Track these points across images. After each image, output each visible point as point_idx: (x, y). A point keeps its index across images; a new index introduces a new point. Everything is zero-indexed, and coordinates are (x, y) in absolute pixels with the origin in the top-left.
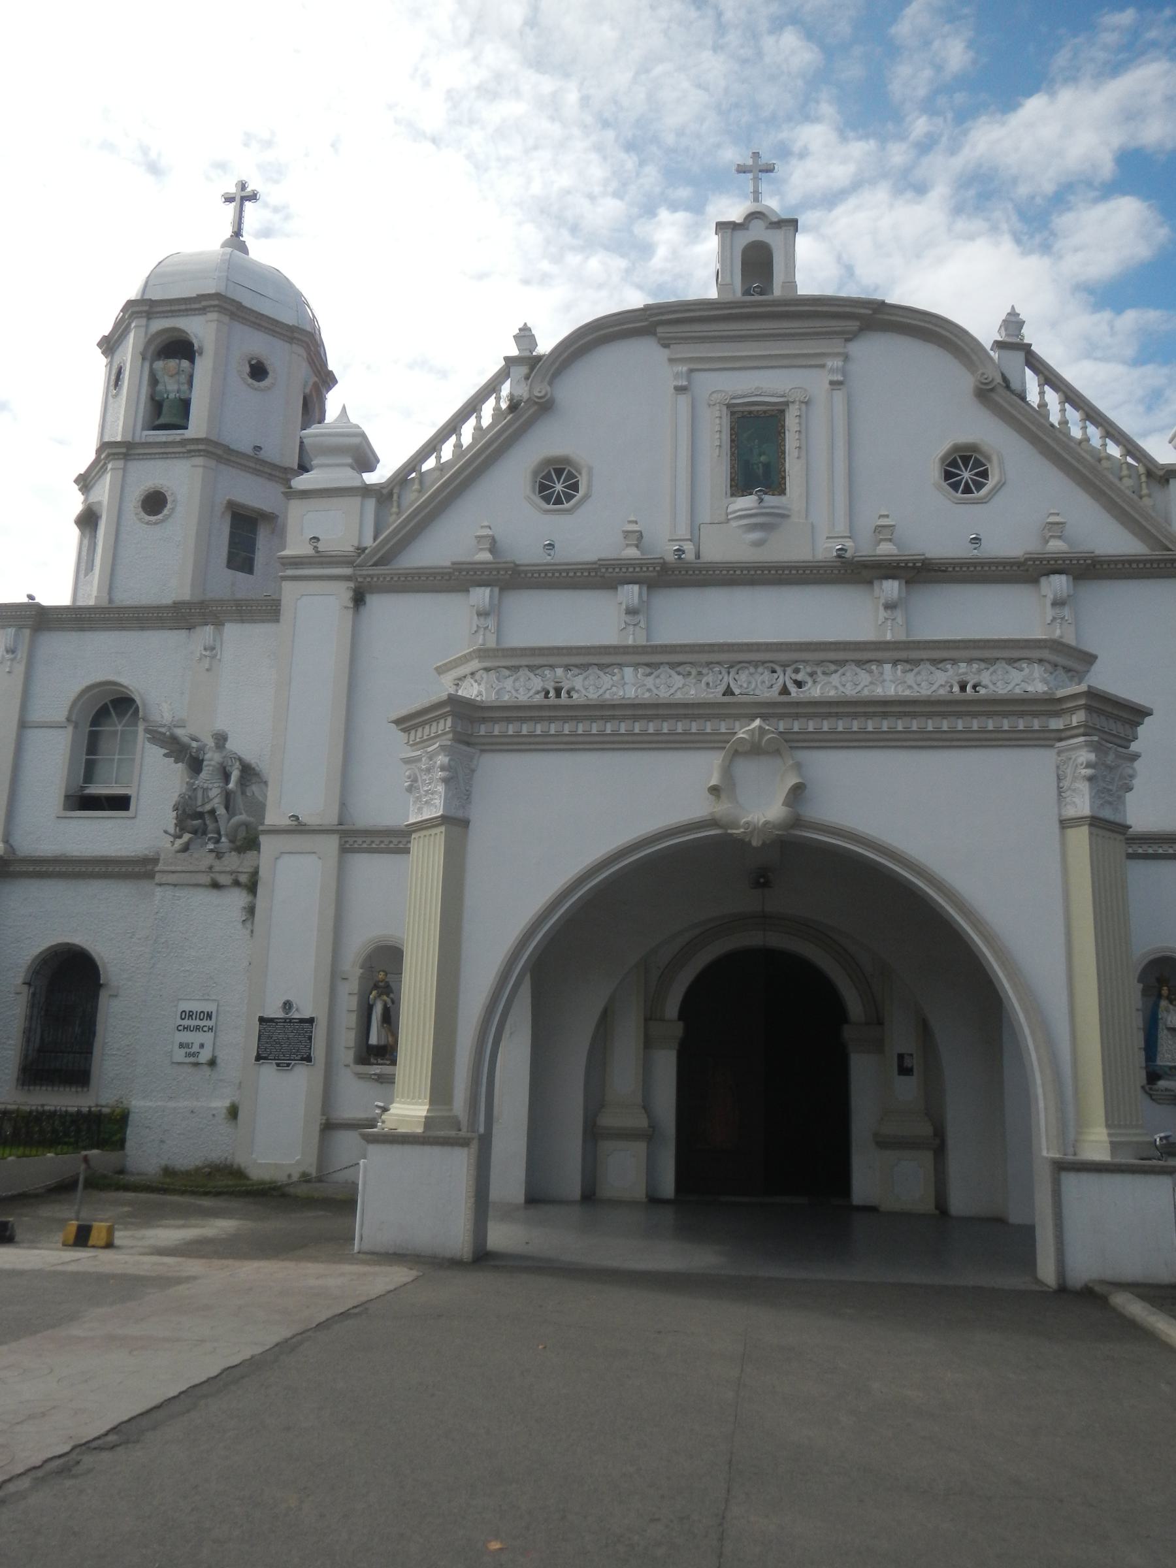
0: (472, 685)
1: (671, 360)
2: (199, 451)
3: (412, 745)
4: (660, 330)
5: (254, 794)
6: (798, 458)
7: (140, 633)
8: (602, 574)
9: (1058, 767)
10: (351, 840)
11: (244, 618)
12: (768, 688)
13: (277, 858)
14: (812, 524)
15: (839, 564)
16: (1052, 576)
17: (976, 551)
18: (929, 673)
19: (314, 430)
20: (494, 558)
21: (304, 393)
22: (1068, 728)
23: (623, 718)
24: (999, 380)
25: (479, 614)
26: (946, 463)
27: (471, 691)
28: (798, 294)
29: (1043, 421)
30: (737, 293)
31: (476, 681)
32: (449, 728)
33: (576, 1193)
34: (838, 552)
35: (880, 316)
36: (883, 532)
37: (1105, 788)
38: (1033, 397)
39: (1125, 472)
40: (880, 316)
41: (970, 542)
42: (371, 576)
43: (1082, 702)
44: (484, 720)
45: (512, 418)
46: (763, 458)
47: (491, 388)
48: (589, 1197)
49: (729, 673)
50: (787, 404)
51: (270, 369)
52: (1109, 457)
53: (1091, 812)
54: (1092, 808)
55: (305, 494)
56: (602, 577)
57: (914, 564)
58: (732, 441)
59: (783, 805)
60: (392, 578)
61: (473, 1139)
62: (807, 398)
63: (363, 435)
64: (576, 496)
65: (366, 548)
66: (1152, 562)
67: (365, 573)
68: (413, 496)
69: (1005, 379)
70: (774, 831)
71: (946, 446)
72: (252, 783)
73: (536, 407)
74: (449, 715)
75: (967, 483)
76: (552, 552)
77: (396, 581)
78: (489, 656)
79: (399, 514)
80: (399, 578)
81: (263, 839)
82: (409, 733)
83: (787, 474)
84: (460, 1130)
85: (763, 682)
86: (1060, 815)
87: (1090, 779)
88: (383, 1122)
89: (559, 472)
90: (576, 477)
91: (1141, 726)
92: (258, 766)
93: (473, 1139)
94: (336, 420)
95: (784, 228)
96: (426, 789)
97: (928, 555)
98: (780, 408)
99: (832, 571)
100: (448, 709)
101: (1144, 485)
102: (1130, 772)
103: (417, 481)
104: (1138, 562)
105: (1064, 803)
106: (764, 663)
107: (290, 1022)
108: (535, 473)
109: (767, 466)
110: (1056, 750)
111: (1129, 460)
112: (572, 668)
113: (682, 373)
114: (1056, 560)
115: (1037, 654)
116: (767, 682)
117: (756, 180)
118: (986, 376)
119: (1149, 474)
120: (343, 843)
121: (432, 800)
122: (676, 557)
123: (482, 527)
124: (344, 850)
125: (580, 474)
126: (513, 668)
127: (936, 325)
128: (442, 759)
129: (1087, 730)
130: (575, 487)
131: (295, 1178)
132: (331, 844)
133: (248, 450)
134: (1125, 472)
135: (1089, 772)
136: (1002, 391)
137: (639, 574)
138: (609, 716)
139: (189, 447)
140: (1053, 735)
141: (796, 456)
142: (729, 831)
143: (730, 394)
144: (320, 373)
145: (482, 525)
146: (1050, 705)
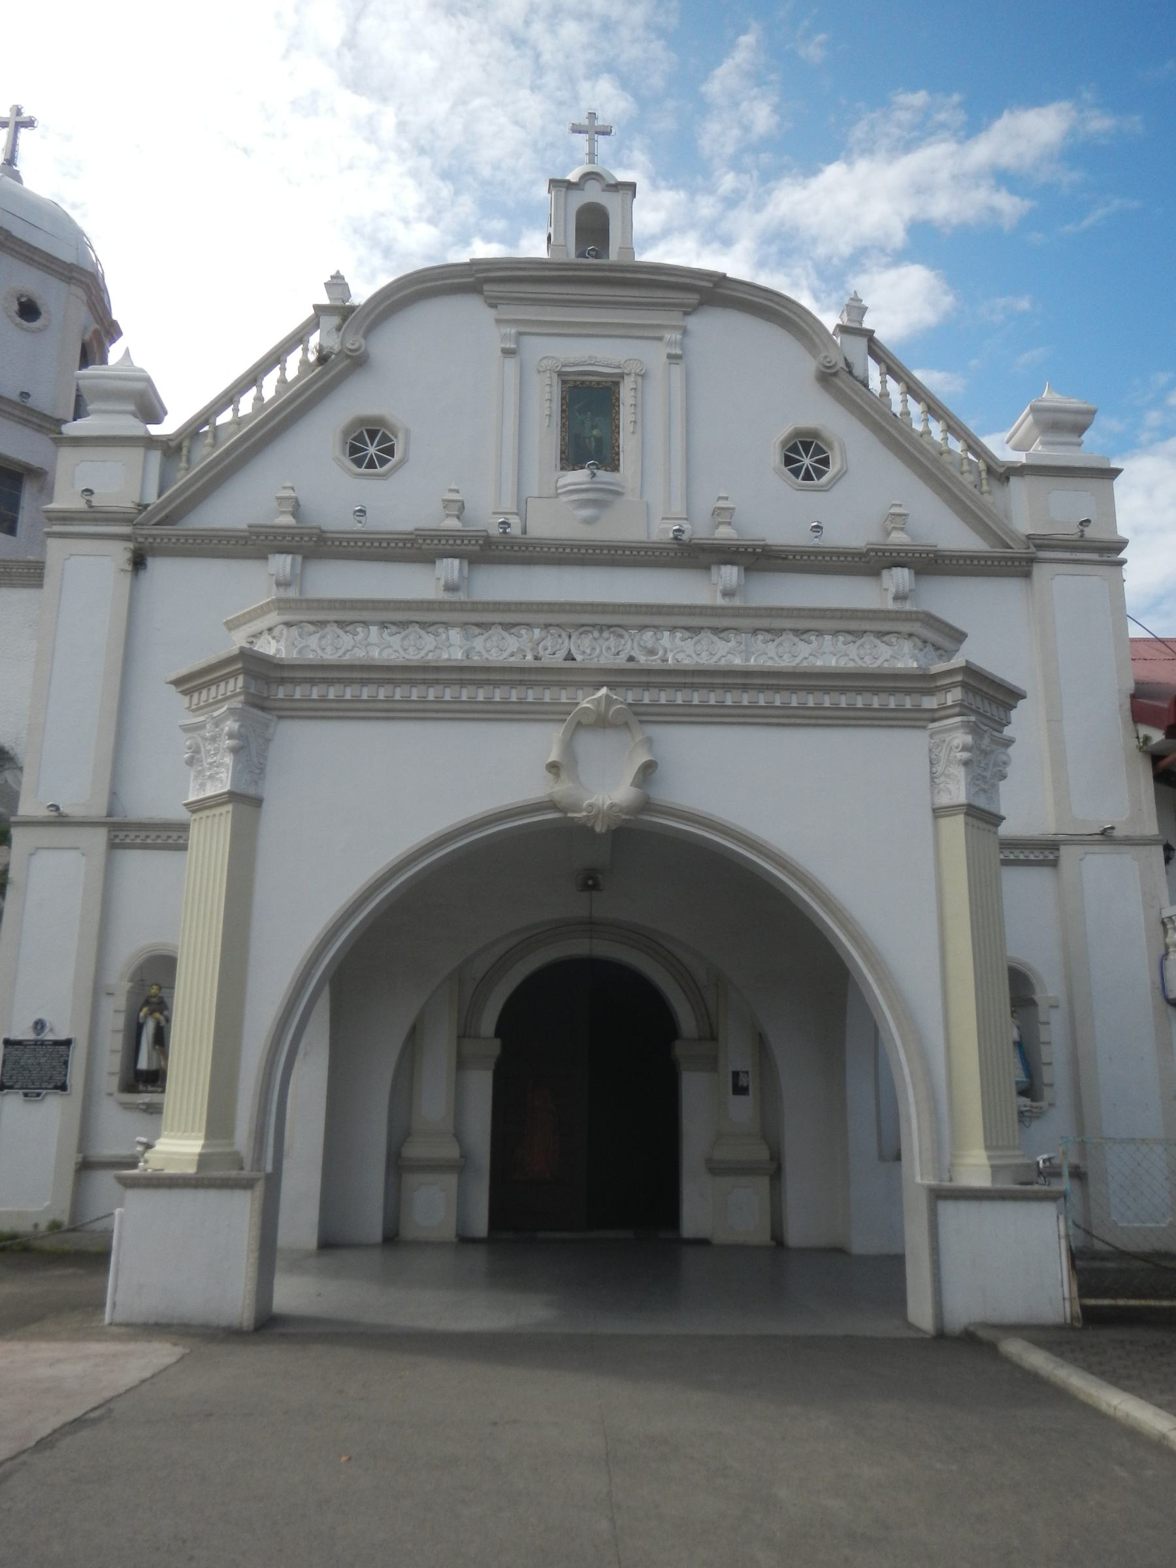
0: (269, 643)
1: (498, 321)
3: (194, 711)
4: (486, 287)
5: (6, 781)
6: (633, 433)
8: (418, 546)
9: (930, 751)
10: (122, 835)
12: (614, 655)
13: (32, 855)
14: (648, 506)
15: (676, 546)
16: (894, 568)
17: (816, 539)
18: (792, 643)
19: (91, 370)
20: (297, 522)
21: (83, 340)
22: (943, 707)
23: (448, 683)
24: (842, 364)
25: (279, 584)
26: (786, 449)
27: (269, 647)
28: (636, 260)
29: (886, 409)
30: (570, 253)
31: (274, 638)
32: (240, 688)
33: (377, 1234)
34: (676, 533)
35: (720, 290)
36: (722, 514)
37: (979, 774)
38: (875, 383)
39: (966, 467)
40: (720, 290)
41: (811, 530)
42: (154, 537)
43: (959, 678)
44: (282, 681)
45: (321, 370)
46: (595, 432)
47: (298, 338)
48: (392, 1238)
49: (570, 637)
50: (622, 376)
51: (42, 309)
52: (950, 452)
53: (966, 799)
54: (968, 797)
55: (78, 442)
56: (420, 549)
57: (755, 549)
58: (563, 411)
59: (631, 786)
60: (178, 540)
61: (259, 1179)
62: (644, 370)
63: (148, 380)
64: (390, 460)
65: (148, 505)
66: (993, 559)
67: (143, 532)
68: (206, 450)
69: (848, 364)
70: (620, 814)
71: (785, 431)
72: (5, 769)
73: (346, 362)
74: (240, 673)
75: (807, 470)
77: (183, 543)
78: (290, 608)
79: (187, 470)
80: (187, 540)
81: (16, 834)
82: (191, 697)
83: (621, 449)
84: (242, 1168)
85: (609, 648)
86: (933, 804)
87: (966, 763)
88: (146, 1162)
89: (372, 434)
90: (392, 441)
91: (1015, 710)
92: (12, 749)
93: (259, 1179)
94: (117, 363)
95: (621, 192)
96: (210, 760)
97: (769, 541)
98: (614, 379)
99: (668, 553)
100: (239, 665)
101: (984, 482)
102: (1005, 758)
103: (210, 435)
104: (979, 558)
105: (936, 791)
106: (609, 627)
107: (42, 1044)
108: (346, 432)
109: (599, 441)
110: (927, 733)
111: (971, 456)
112: (389, 625)
113: (510, 334)
114: (898, 552)
115: (905, 627)
116: (613, 649)
117: (592, 141)
118: (829, 360)
119: (990, 470)
120: (112, 838)
121: (217, 773)
122: (501, 530)
123: (284, 488)
124: (113, 846)
125: (396, 437)
126: (319, 624)
127: (778, 304)
128: (231, 725)
129: (964, 708)
130: (390, 451)
131: (43, 1226)
132: (99, 838)
133: (15, 397)
134: (966, 467)
135: (965, 755)
137: (460, 547)
138: (433, 679)
140: (926, 715)
141: (632, 430)
142: (570, 815)
143: (562, 360)
144: (101, 320)
145: (284, 485)
146: (923, 683)
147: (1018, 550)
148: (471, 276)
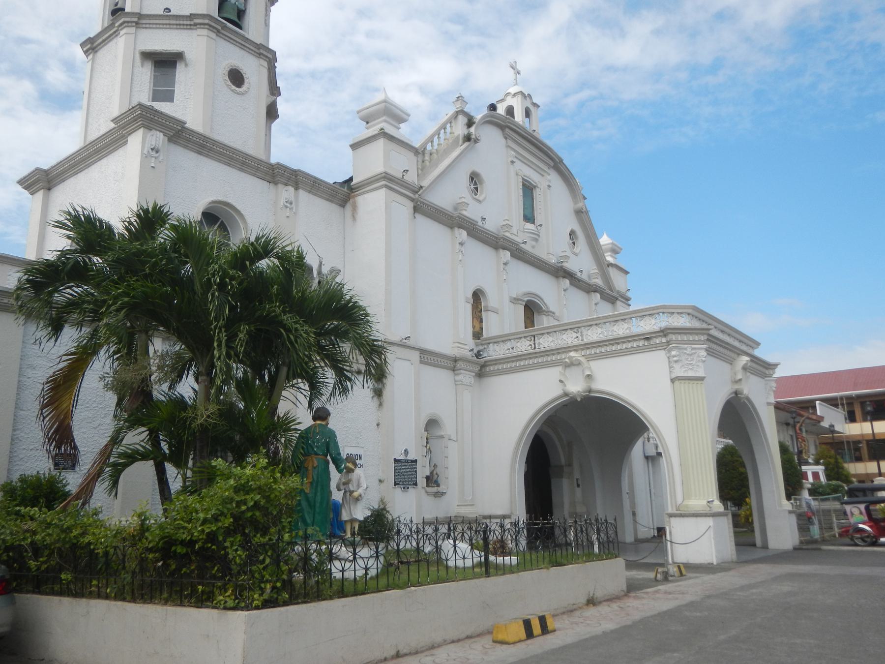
2: (266, 57)
4: (507, 130)
7: (239, 172)
11: (312, 191)
76: (484, 222)
136: (585, 214)
139: (261, 51)
147: (615, 294)
148: (505, 123)
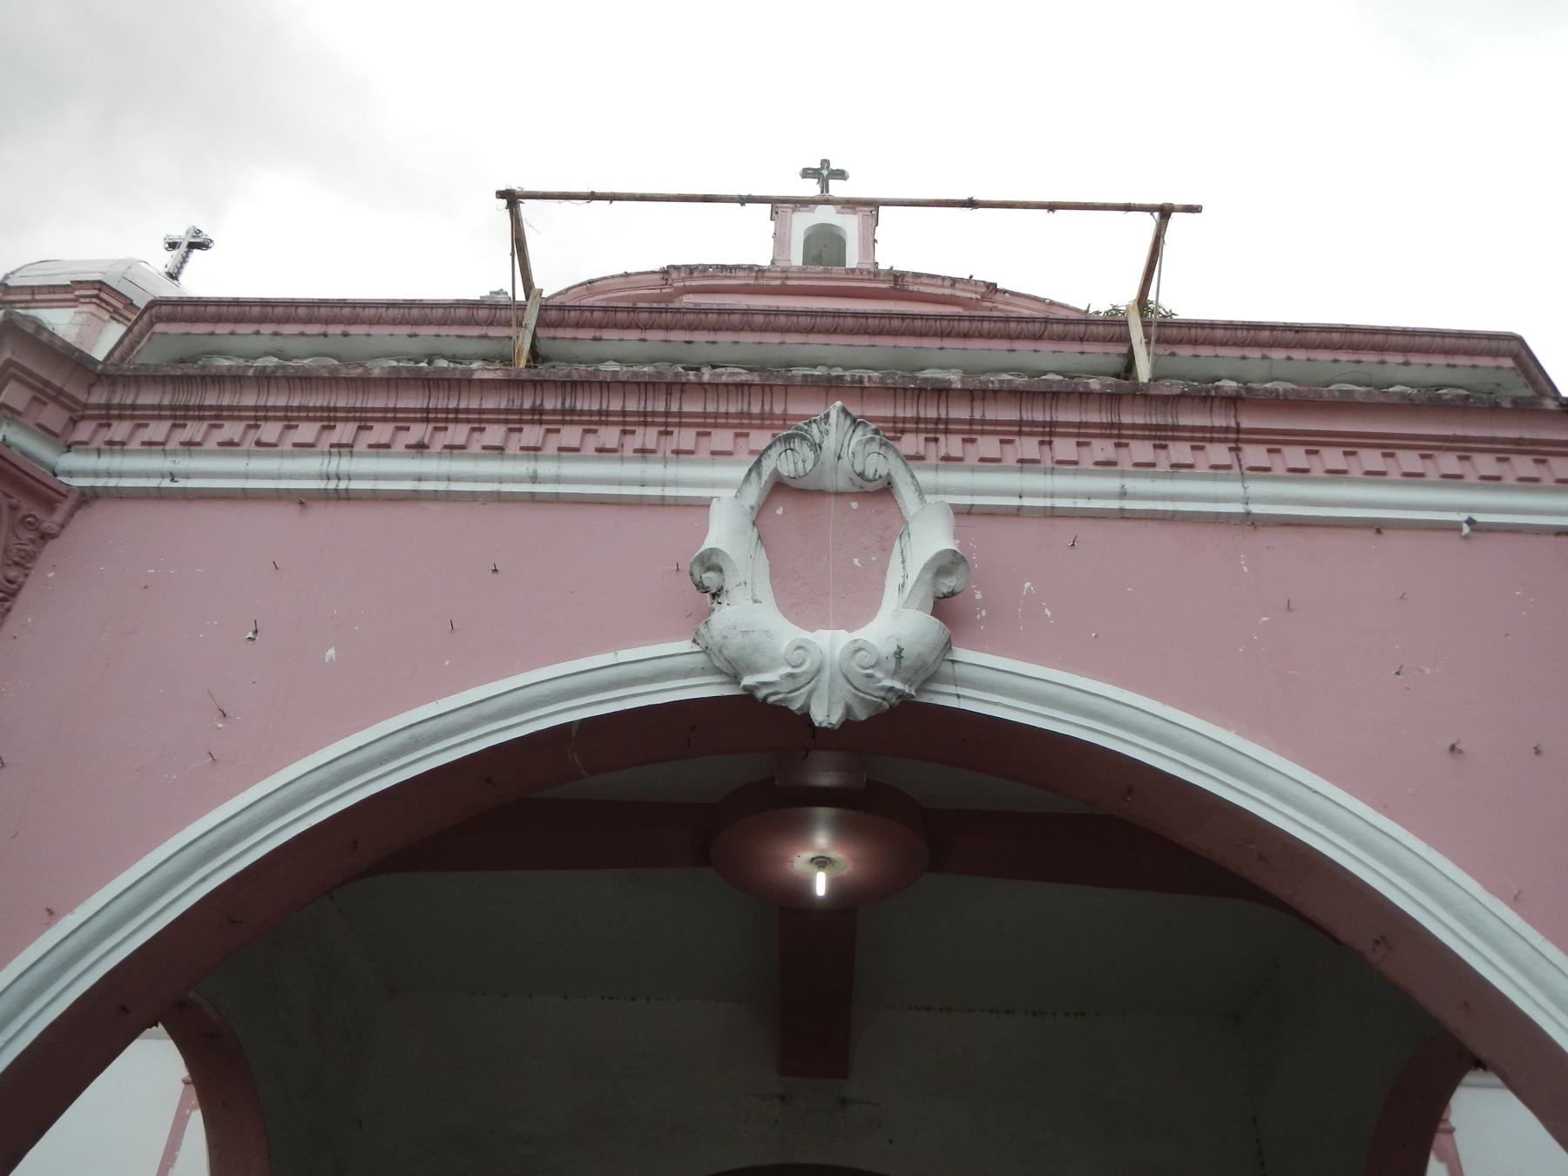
70: (879, 675)
142: (748, 680)
